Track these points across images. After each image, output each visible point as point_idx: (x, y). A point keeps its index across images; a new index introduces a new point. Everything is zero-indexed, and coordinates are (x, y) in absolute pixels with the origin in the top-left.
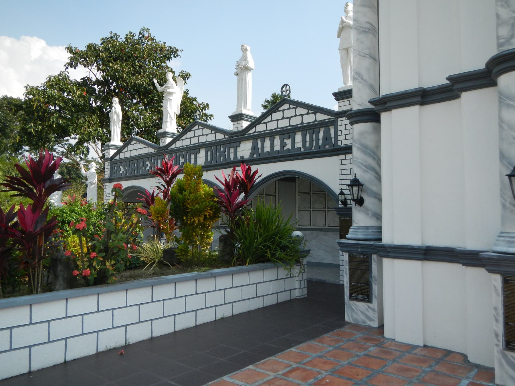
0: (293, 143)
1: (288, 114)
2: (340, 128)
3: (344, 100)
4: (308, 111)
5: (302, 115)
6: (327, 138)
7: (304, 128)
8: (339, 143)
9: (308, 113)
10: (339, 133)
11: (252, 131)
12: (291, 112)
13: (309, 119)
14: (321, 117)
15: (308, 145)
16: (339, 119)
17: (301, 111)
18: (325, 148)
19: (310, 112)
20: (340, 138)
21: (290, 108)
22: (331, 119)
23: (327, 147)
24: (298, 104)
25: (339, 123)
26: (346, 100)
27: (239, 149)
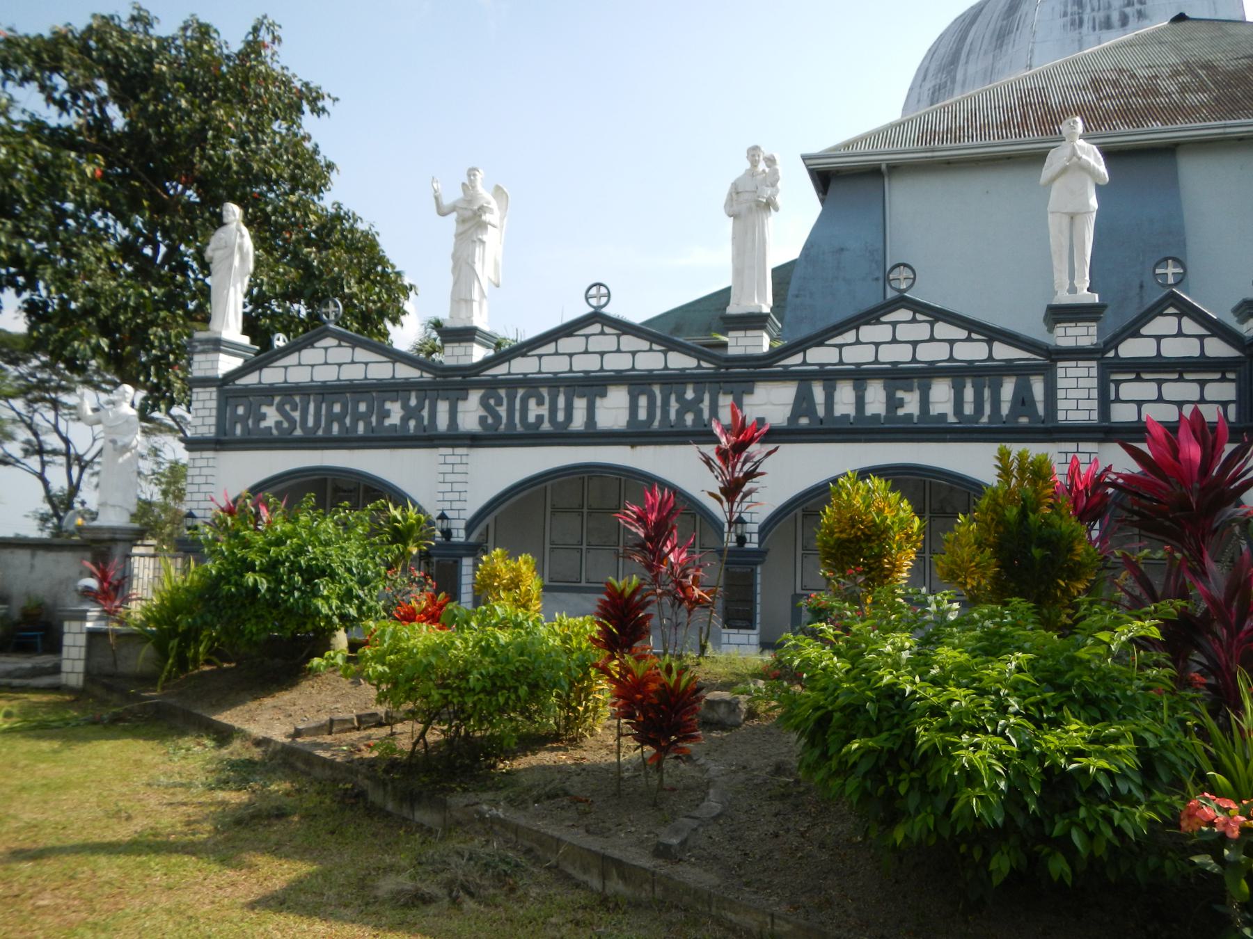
0: (925, 402)
1: (904, 332)
2: (1061, 383)
3: (1074, 324)
4: (969, 334)
5: (951, 342)
6: (1023, 400)
7: (958, 373)
8: (1061, 416)
9: (969, 339)
10: (1061, 394)
11: (797, 359)
12: (922, 331)
13: (974, 351)
14: (1003, 352)
15: (968, 409)
16: (1060, 364)
17: (943, 330)
18: (1017, 422)
19: (974, 336)
20: (1061, 405)
21: (914, 321)
22: (1034, 359)
23: (1024, 420)
24: (937, 315)
25: (1060, 373)
26: (1079, 324)
27: (747, 400)
